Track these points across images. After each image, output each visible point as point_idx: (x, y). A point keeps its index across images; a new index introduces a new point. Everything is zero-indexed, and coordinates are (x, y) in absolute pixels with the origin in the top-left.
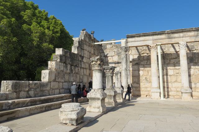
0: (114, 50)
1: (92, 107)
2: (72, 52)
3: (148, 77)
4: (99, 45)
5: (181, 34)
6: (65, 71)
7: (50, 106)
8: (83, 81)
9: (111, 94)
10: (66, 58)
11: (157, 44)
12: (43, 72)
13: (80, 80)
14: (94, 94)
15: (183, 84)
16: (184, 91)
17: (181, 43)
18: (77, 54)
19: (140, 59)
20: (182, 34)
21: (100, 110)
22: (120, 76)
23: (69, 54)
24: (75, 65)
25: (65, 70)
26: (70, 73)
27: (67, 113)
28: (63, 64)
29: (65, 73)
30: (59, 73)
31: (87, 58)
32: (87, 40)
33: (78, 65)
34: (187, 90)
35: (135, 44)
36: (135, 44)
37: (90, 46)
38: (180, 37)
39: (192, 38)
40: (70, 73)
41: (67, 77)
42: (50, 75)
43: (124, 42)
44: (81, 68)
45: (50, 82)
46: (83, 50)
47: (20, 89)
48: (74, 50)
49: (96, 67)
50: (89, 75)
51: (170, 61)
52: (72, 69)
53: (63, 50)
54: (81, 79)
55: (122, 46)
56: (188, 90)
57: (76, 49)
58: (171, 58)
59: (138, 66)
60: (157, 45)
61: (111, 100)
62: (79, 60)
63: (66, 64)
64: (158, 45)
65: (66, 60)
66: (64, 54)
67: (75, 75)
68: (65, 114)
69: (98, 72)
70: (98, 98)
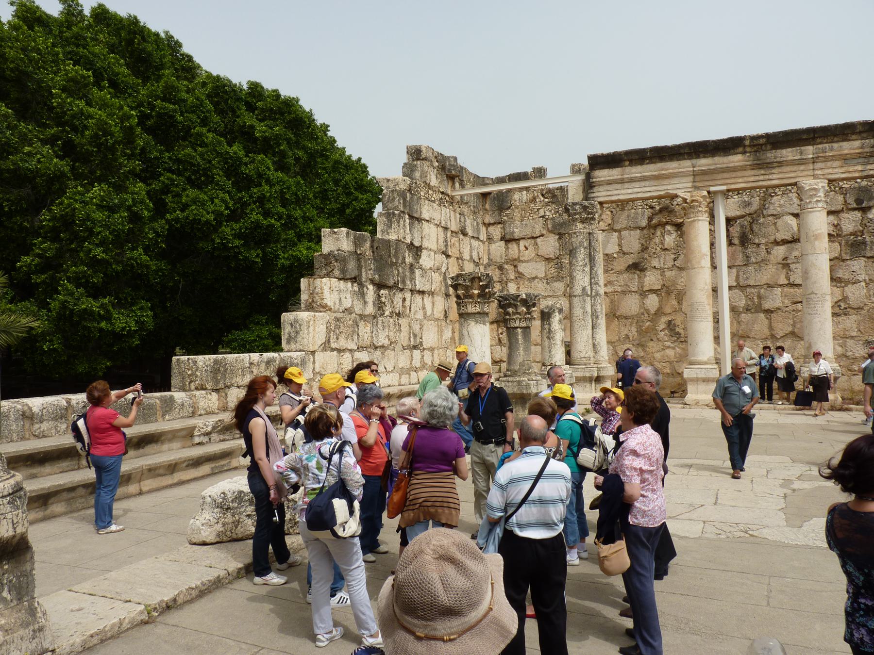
2: (379, 235)
3: (678, 319)
5: (809, 151)
6: (358, 308)
8: (421, 343)
9: (525, 392)
10: (360, 262)
11: (712, 189)
13: (412, 339)
17: (807, 183)
19: (647, 248)
24: (391, 282)
26: (375, 317)
28: (349, 284)
30: (337, 319)
31: (435, 253)
32: (434, 181)
33: (404, 282)
35: (622, 192)
36: (622, 192)
38: (801, 162)
39: (856, 161)
40: (375, 317)
45: (313, 353)
46: (419, 220)
47: (228, 380)
49: (469, 307)
50: (446, 316)
51: (768, 253)
53: (348, 233)
54: (415, 336)
58: (772, 238)
59: (639, 277)
60: (709, 192)
62: (404, 262)
63: (361, 285)
64: (716, 193)
65: (360, 268)
67: (391, 320)
69: (477, 322)
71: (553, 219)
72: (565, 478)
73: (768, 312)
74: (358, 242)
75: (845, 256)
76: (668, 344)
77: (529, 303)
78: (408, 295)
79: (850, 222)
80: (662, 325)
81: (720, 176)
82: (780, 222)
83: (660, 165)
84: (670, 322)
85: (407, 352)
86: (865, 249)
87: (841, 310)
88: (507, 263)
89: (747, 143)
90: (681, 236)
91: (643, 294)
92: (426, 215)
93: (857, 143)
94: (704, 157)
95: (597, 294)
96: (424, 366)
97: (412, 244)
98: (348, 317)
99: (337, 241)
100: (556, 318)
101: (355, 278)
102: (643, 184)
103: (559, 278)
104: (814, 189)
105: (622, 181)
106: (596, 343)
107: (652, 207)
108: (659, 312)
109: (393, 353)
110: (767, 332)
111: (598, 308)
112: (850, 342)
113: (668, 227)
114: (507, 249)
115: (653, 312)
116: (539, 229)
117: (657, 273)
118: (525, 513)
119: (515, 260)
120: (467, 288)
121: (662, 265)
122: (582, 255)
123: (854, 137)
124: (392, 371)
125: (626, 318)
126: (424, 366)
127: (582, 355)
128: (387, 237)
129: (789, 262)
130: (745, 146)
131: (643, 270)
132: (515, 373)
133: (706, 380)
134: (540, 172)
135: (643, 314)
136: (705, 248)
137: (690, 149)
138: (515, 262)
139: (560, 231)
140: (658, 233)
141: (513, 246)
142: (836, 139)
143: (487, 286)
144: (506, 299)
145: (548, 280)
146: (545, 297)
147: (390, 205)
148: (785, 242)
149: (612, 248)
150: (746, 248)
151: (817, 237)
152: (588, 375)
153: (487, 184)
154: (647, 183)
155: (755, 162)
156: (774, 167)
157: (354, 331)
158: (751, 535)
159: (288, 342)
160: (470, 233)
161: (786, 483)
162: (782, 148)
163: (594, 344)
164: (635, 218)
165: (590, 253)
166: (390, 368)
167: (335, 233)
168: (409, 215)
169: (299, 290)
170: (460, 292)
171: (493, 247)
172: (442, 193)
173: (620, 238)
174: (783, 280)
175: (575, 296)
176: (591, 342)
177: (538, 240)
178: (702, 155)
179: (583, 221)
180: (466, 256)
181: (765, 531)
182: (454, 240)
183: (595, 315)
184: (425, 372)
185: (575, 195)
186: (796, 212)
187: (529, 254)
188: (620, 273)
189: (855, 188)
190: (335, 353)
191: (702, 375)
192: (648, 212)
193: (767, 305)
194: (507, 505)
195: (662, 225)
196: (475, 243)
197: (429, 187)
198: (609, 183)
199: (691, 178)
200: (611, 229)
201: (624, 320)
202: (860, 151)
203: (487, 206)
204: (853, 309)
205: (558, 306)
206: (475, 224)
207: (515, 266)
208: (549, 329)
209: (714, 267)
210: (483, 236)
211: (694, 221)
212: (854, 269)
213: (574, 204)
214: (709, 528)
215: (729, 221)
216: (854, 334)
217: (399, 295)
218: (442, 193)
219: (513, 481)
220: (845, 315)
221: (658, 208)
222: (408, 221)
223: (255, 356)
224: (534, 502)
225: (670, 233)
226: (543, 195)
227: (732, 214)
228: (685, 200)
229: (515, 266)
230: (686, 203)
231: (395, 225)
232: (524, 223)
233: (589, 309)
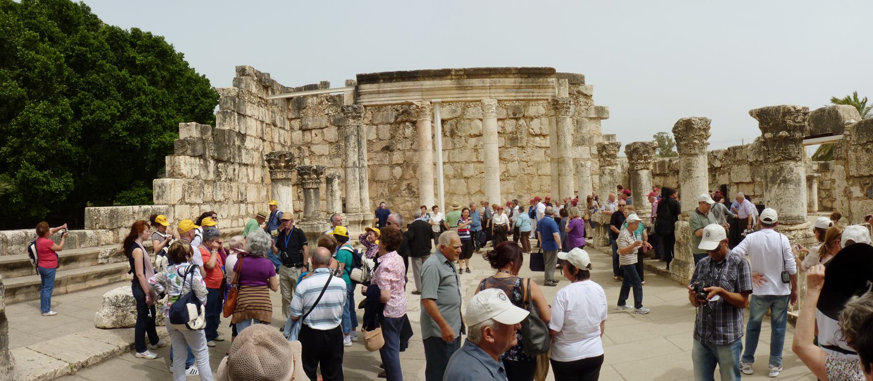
2: (217, 127)
3: (414, 183)
5: (488, 81)
6: (203, 177)
8: (246, 199)
11: (433, 100)
17: (487, 101)
20: (488, 80)
23: (210, 133)
24: (226, 158)
26: (215, 182)
28: (198, 160)
30: (190, 183)
33: (234, 158)
38: (483, 88)
46: (244, 116)
50: (262, 181)
51: (466, 142)
53: (196, 126)
54: (242, 194)
58: (468, 133)
63: (205, 160)
64: (435, 103)
65: (204, 148)
72: (342, 289)
73: (466, 178)
74: (203, 132)
77: (318, 172)
78: (237, 167)
79: (510, 125)
80: (404, 187)
81: (437, 93)
82: (472, 124)
83: (402, 83)
85: (237, 205)
87: (505, 177)
89: (453, 73)
90: (415, 129)
91: (392, 166)
92: (249, 113)
93: (512, 80)
95: (363, 166)
96: (248, 215)
99: (189, 131)
100: (336, 182)
102: (392, 95)
103: (338, 155)
105: (378, 93)
107: (397, 110)
108: (402, 178)
110: (466, 191)
111: (364, 175)
113: (407, 124)
114: (304, 135)
116: (324, 122)
117: (400, 153)
118: (316, 313)
120: (276, 162)
122: (353, 140)
125: (382, 182)
126: (248, 215)
128: (223, 128)
131: (392, 151)
132: (309, 219)
134: (325, 85)
138: (309, 145)
139: (339, 124)
140: (401, 127)
141: (308, 134)
143: (290, 161)
145: (331, 157)
146: (329, 168)
147: (225, 106)
148: (476, 136)
149: (373, 136)
151: (492, 134)
152: (357, 220)
153: (290, 92)
160: (278, 123)
163: (361, 200)
164: (387, 117)
166: (225, 216)
169: (165, 164)
170: (272, 165)
171: (294, 134)
173: (377, 129)
174: (475, 160)
179: (353, 118)
180: (276, 140)
182: (268, 129)
183: (361, 180)
184: (249, 219)
185: (348, 100)
187: (319, 139)
188: (377, 152)
192: (395, 113)
193: (466, 174)
194: (304, 308)
195: (404, 122)
196: (282, 131)
197: (251, 93)
198: (371, 93)
200: (372, 123)
203: (290, 107)
208: (332, 191)
209: (434, 149)
210: (287, 127)
213: (348, 106)
215: (443, 121)
217: (231, 167)
219: (308, 292)
224: (322, 305)
225: (408, 128)
227: (445, 117)
228: (418, 107)
231: (228, 120)
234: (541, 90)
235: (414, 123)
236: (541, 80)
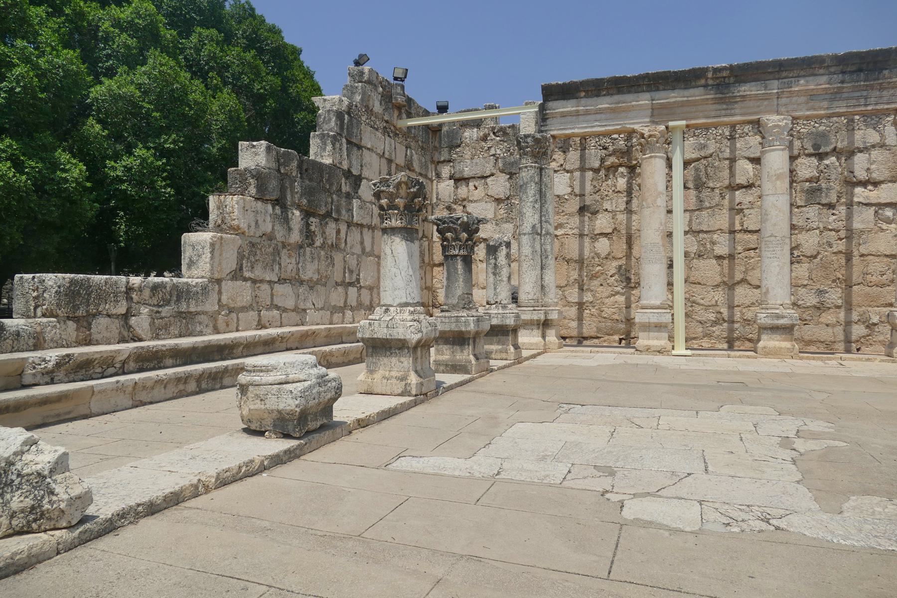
0: (492, 152)
1: (378, 376)
4: (427, 127)
6: (280, 234)
7: (217, 373)
8: (358, 280)
11: (671, 124)
12: (188, 238)
14: (384, 325)
15: (767, 290)
16: (769, 321)
17: (772, 120)
18: (334, 167)
21: (409, 389)
22: (508, 255)
23: (295, 164)
24: (322, 211)
25: (281, 234)
26: (301, 247)
27: (261, 391)
28: (270, 207)
29: (280, 245)
30: (253, 245)
33: (338, 212)
34: (779, 317)
37: (390, 131)
38: (766, 98)
40: (301, 247)
41: (288, 262)
42: (217, 254)
43: (533, 116)
44: (349, 225)
45: (219, 281)
46: (360, 147)
47: (92, 307)
48: (321, 152)
52: (313, 228)
53: (268, 149)
55: (522, 133)
56: (783, 317)
57: (329, 147)
60: (667, 127)
61: (462, 351)
62: (341, 190)
63: (284, 208)
64: (675, 128)
65: (283, 190)
66: (274, 165)
67: (323, 253)
68: (257, 396)
70: (400, 340)
71: (504, 158)
75: (800, 203)
76: (619, 289)
78: (343, 227)
79: (807, 168)
83: (617, 98)
84: (620, 266)
85: (340, 289)
86: (821, 197)
88: (455, 202)
89: (710, 75)
92: (367, 142)
94: (664, 90)
95: (548, 233)
97: (349, 171)
98: (266, 243)
99: (253, 156)
100: (503, 251)
101: (276, 200)
102: (598, 117)
103: (507, 220)
104: (778, 126)
106: (545, 284)
107: (605, 148)
109: (323, 288)
111: (548, 247)
112: (802, 291)
115: (603, 256)
117: (608, 216)
119: (464, 200)
121: (614, 208)
123: (821, 71)
124: (322, 309)
127: (530, 297)
128: (319, 159)
129: (743, 207)
130: (707, 79)
131: (595, 213)
133: (659, 327)
135: (593, 258)
136: (662, 186)
137: (650, 80)
142: (802, 73)
144: (444, 223)
147: (326, 127)
150: (700, 192)
152: (536, 318)
154: (603, 116)
155: (717, 96)
156: (736, 102)
157: (274, 261)
158: (777, 528)
159: (189, 267)
161: (786, 442)
162: (745, 82)
163: (543, 287)
165: (541, 189)
167: (254, 146)
168: (347, 140)
170: (384, 202)
172: (387, 122)
175: (525, 234)
176: (539, 283)
177: (489, 180)
178: (661, 87)
181: (794, 518)
183: (544, 255)
185: (528, 127)
186: (752, 156)
188: (571, 215)
189: (812, 133)
190: (249, 284)
191: (654, 319)
197: (369, 111)
198: (563, 115)
199: (649, 112)
200: (563, 169)
201: (573, 264)
202: (827, 86)
204: (808, 257)
205: (505, 239)
206: (423, 160)
207: (464, 207)
208: (495, 264)
211: (651, 157)
212: (808, 216)
213: (526, 136)
214: (711, 515)
215: (686, 164)
216: (805, 282)
218: (387, 122)
220: (798, 262)
221: (611, 149)
222: (345, 146)
223: (135, 280)
225: (623, 176)
226: (494, 133)
227: (689, 156)
229: (464, 207)
230: (643, 138)
232: (474, 161)
233: (538, 248)
234: (885, 93)
235: (632, 169)
236: (886, 72)
